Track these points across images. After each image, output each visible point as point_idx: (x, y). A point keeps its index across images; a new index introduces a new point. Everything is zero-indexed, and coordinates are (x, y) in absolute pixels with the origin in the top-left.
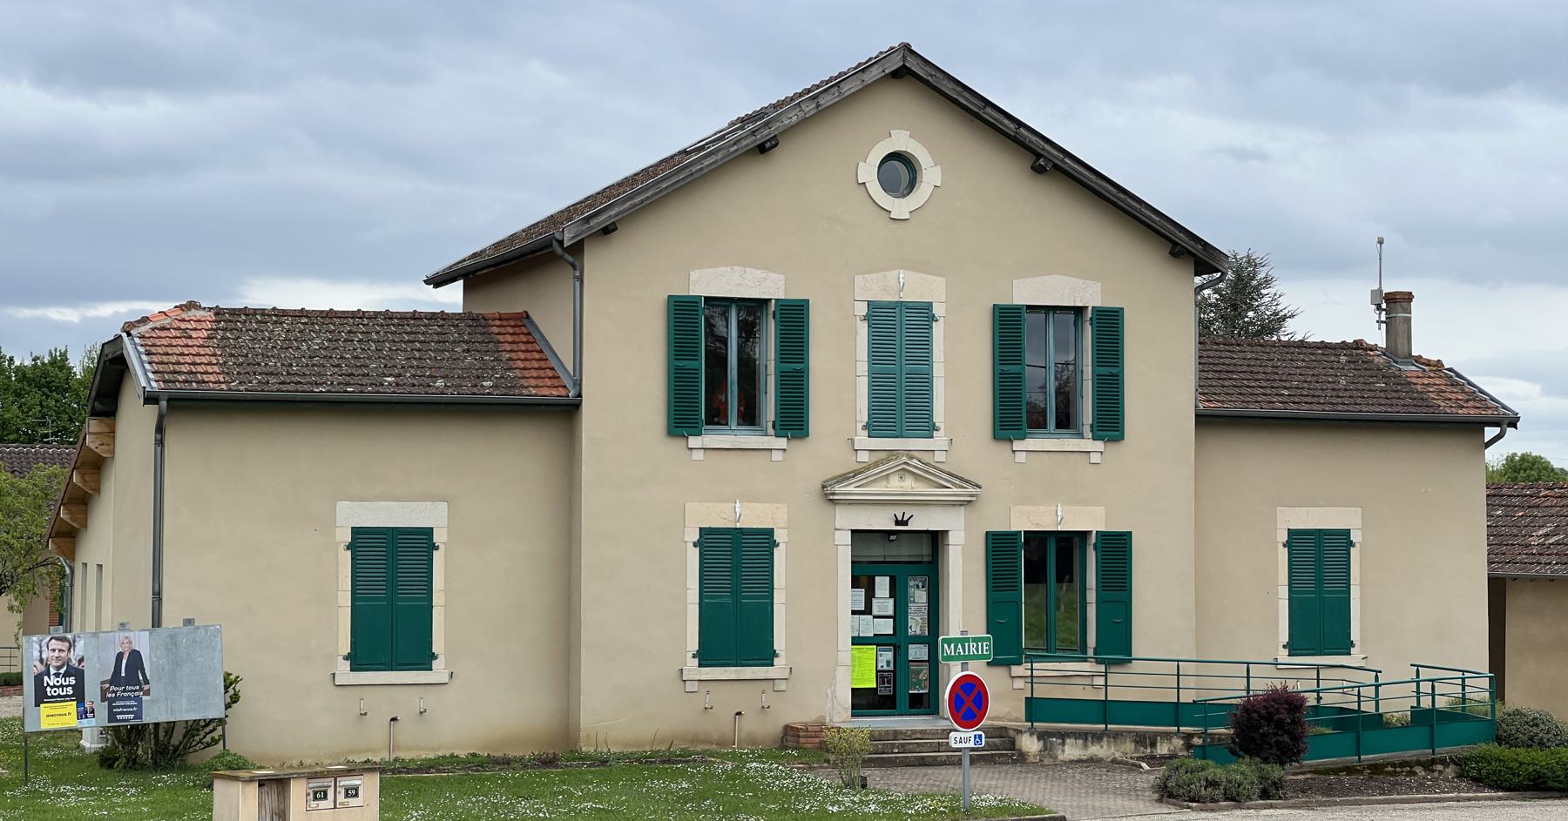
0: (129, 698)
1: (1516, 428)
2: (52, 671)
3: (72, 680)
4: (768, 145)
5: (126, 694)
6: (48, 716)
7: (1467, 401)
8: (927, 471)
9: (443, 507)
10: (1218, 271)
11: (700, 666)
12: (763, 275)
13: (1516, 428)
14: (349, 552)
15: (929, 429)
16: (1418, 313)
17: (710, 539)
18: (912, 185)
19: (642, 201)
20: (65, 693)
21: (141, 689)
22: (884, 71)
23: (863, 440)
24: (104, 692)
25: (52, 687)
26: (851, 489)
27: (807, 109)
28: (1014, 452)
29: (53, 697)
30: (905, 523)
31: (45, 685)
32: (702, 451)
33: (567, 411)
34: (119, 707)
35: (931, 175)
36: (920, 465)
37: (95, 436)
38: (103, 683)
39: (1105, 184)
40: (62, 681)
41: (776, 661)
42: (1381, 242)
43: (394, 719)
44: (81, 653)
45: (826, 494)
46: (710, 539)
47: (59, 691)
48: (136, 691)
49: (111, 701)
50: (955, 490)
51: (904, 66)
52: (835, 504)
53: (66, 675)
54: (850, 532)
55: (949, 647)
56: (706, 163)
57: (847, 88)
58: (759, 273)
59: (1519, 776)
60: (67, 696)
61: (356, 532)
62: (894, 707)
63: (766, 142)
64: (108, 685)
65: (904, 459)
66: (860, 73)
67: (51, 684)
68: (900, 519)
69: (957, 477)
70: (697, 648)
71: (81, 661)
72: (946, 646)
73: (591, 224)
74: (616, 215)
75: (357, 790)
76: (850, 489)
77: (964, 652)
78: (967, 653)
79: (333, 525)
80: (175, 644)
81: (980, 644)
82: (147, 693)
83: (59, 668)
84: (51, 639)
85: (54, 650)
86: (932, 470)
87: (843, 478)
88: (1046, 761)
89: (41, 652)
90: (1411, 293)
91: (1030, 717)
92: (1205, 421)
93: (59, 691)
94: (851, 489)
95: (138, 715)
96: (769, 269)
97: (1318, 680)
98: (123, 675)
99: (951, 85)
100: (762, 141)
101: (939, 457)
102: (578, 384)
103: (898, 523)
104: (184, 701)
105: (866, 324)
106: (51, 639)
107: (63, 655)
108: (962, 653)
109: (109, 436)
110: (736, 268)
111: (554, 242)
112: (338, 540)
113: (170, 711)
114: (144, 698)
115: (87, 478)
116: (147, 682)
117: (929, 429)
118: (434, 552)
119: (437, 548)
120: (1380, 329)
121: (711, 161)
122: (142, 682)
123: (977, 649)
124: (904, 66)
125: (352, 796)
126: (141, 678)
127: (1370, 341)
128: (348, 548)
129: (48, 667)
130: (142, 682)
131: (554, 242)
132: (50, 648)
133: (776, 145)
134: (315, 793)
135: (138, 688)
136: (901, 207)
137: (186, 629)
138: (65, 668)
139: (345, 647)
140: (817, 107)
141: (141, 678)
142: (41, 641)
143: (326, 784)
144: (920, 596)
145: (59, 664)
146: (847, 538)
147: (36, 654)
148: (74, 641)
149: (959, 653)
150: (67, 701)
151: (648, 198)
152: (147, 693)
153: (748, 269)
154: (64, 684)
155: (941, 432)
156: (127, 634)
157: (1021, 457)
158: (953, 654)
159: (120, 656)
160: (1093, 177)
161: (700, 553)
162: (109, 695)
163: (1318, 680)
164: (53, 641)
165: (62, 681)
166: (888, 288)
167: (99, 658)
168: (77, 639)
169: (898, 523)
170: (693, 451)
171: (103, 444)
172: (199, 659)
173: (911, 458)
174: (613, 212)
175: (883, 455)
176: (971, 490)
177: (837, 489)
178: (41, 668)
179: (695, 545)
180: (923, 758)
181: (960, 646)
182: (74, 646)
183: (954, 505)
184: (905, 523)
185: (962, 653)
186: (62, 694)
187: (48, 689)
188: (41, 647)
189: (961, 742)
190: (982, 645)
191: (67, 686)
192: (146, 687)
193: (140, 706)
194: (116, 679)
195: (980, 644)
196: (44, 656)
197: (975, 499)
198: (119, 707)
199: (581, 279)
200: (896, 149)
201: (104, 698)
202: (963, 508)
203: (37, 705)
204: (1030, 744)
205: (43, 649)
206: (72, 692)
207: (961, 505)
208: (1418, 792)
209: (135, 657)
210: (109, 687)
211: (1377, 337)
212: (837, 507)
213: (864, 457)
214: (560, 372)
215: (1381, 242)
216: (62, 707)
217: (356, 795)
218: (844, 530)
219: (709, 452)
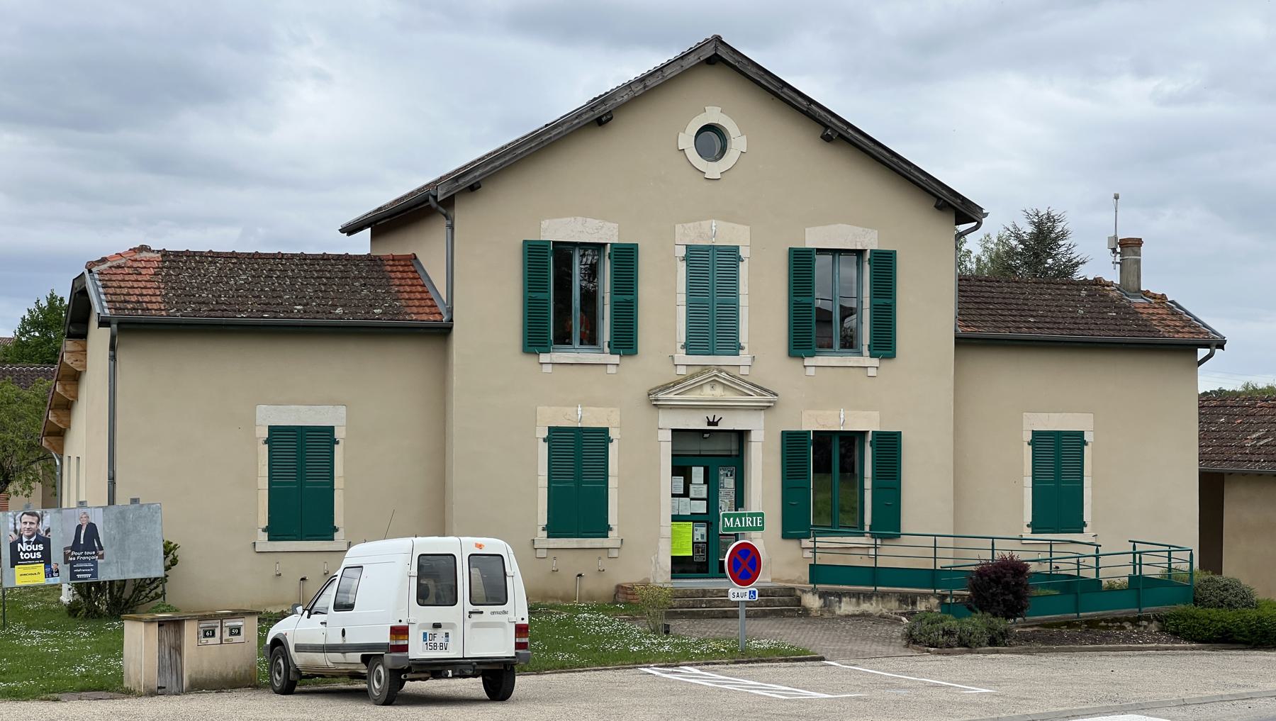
0: (87, 561)
1: (1223, 349)
2: (25, 539)
3: (41, 547)
4: (604, 119)
5: (84, 558)
7: (1183, 327)
8: (734, 382)
9: (342, 410)
10: (974, 221)
11: (548, 537)
12: (601, 224)
13: (1223, 349)
15: (736, 349)
17: (557, 436)
18: (723, 151)
19: (501, 165)
20: (35, 557)
21: (96, 554)
23: (681, 357)
24: (66, 556)
25: (24, 552)
26: (671, 396)
27: (636, 90)
28: (805, 366)
29: (25, 560)
30: (716, 424)
31: (19, 550)
33: (442, 332)
34: (79, 568)
35: (738, 143)
37: (70, 354)
38: (65, 549)
39: (880, 150)
40: (32, 547)
41: (610, 533)
42: (1117, 197)
43: (303, 579)
44: (48, 525)
45: (651, 401)
46: (557, 436)
47: (30, 555)
48: (91, 555)
49: (72, 563)
50: (756, 397)
51: (716, 54)
52: (659, 408)
53: (36, 543)
55: (729, 520)
56: (554, 134)
57: (669, 72)
58: (597, 223)
59: (1209, 630)
60: (36, 559)
61: (273, 430)
62: (707, 572)
63: (602, 116)
64: (69, 551)
65: (715, 372)
66: (679, 60)
67: (24, 550)
68: (711, 420)
69: (758, 387)
70: (546, 523)
71: (48, 531)
72: (726, 519)
73: (460, 183)
74: (480, 175)
75: (239, 629)
76: (671, 396)
77: (741, 524)
78: (743, 526)
79: (253, 424)
80: (124, 519)
81: (754, 518)
82: (102, 557)
83: (30, 537)
84: (23, 515)
85: (26, 523)
86: (737, 381)
87: (665, 388)
88: (826, 615)
89: (15, 524)
90: (1141, 239)
91: (813, 580)
92: (962, 342)
93: (30, 555)
94: (671, 396)
95: (94, 574)
96: (605, 219)
97: (1051, 552)
98: (82, 542)
99: (755, 70)
100: (599, 116)
101: (744, 371)
102: (451, 311)
103: (710, 424)
104: (131, 563)
105: (684, 264)
106: (23, 515)
107: (33, 526)
108: (740, 526)
109: (82, 354)
111: (430, 198)
112: (257, 436)
113: (120, 571)
114: (99, 561)
115: (68, 388)
116: (101, 548)
117: (736, 349)
118: (335, 446)
119: (338, 443)
120: (1115, 269)
121: (560, 130)
122: (97, 548)
123: (752, 522)
124: (716, 54)
125: (235, 634)
126: (96, 545)
127: (1108, 279)
128: (266, 443)
129: (21, 536)
130: (97, 548)
131: (430, 198)
132: (23, 521)
133: (611, 118)
134: (205, 632)
135: (94, 553)
136: (713, 169)
137: (133, 506)
138: (35, 537)
139: (264, 521)
140: (645, 87)
141: (96, 545)
142: (15, 516)
143: (213, 625)
144: (729, 483)
145: (30, 534)
146: (668, 436)
147: (11, 526)
148: (42, 516)
149: (737, 525)
150: (37, 563)
151: (505, 162)
152: (102, 557)
153: (588, 219)
154: (34, 550)
155: (746, 351)
156: (85, 510)
157: (811, 371)
158: (732, 526)
159: (79, 528)
160: (871, 144)
162: (71, 559)
163: (1051, 552)
164: (25, 515)
165: (32, 547)
166: (703, 235)
167: (62, 530)
168: (45, 514)
169: (710, 424)
170: (544, 366)
171: (77, 361)
172: (143, 531)
173: (721, 371)
174: (477, 174)
175: (698, 369)
176: (769, 397)
177: (660, 396)
178: (16, 537)
179: (544, 440)
180: (725, 611)
181: (738, 519)
182: (42, 520)
183: (755, 409)
184: (716, 424)
185: (740, 526)
186: (32, 557)
187: (21, 554)
188: (15, 521)
189: (738, 596)
190: (756, 519)
191: (36, 552)
192: (100, 553)
193: (96, 567)
194: (76, 546)
195: (754, 518)
196: (18, 528)
197: (772, 404)
198: (79, 568)
199: (452, 227)
200: (710, 122)
201: (66, 562)
202: (763, 411)
203: (13, 566)
204: (812, 602)
205: (17, 522)
206: (40, 556)
208: (1124, 642)
209: (92, 529)
210: (71, 553)
211: (1112, 275)
212: (660, 411)
213: (682, 371)
214: (437, 302)
215: (1117, 197)
216: (33, 568)
217: (239, 633)
218: (666, 429)
219: (556, 366)
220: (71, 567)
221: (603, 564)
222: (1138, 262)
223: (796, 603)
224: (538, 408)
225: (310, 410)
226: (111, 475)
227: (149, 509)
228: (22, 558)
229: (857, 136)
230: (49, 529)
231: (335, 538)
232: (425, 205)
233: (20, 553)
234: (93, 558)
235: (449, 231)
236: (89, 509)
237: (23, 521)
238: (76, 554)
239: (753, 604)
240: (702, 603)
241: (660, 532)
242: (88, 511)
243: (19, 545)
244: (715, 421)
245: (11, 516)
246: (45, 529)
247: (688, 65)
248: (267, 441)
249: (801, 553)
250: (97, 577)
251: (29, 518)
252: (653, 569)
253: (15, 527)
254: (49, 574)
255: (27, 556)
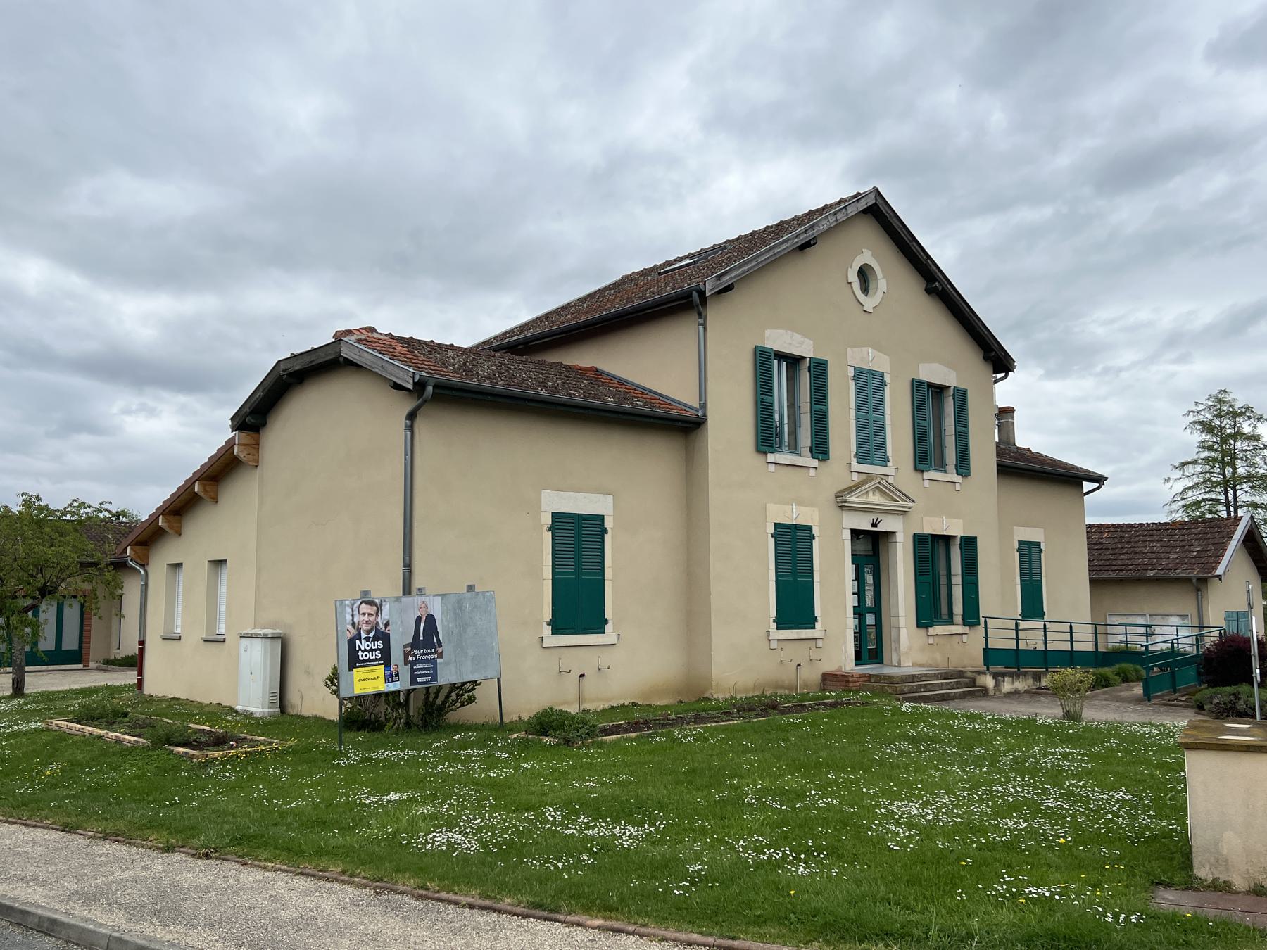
0: (426, 661)
2: (363, 635)
3: (380, 644)
4: (812, 242)
5: (424, 657)
6: (360, 680)
14: (550, 533)
19: (749, 270)
20: (374, 657)
21: (436, 652)
22: (867, 204)
24: (406, 655)
25: (363, 651)
26: (853, 499)
29: (364, 661)
31: (357, 649)
32: (774, 465)
34: (419, 670)
35: (881, 283)
36: (887, 485)
37: (243, 447)
38: (405, 646)
40: (371, 645)
43: (582, 676)
44: (387, 617)
45: (838, 502)
47: (369, 655)
48: (432, 654)
49: (413, 663)
50: (901, 503)
52: (842, 510)
53: (375, 639)
54: (850, 531)
56: (782, 248)
57: (840, 216)
60: (376, 660)
61: (555, 516)
63: (811, 240)
64: (409, 649)
65: (879, 480)
67: (363, 649)
71: (387, 624)
73: (721, 281)
74: (735, 277)
79: (538, 510)
80: (460, 608)
82: (440, 656)
83: (368, 632)
84: (361, 604)
85: (364, 614)
86: (892, 489)
87: (850, 490)
88: (997, 693)
89: (353, 616)
91: (987, 663)
93: (369, 655)
95: (434, 678)
96: (805, 336)
98: (421, 638)
104: (469, 663)
106: (361, 604)
107: (372, 618)
109: (254, 448)
110: (789, 332)
111: (695, 294)
113: (458, 673)
114: (439, 660)
115: (208, 488)
116: (440, 645)
122: (436, 645)
126: (436, 642)
128: (550, 530)
129: (359, 630)
130: (436, 645)
131: (695, 294)
132: (361, 612)
135: (433, 650)
137: (469, 594)
138: (374, 632)
139: (548, 615)
140: (837, 220)
141: (436, 642)
142: (353, 605)
144: (869, 579)
145: (369, 628)
147: (349, 618)
148: (381, 605)
150: (376, 665)
151: (751, 268)
152: (440, 656)
154: (373, 648)
156: (423, 599)
157: (927, 483)
159: (418, 620)
162: (411, 659)
163: (1071, 632)
164: (363, 605)
165: (371, 645)
167: (402, 622)
168: (384, 604)
171: (249, 454)
172: (479, 623)
173: (882, 479)
174: (733, 275)
176: (910, 503)
177: (848, 498)
178: (353, 632)
180: (943, 694)
182: (381, 610)
183: (898, 514)
186: (371, 658)
187: (360, 653)
188: (353, 611)
191: (376, 650)
192: (440, 650)
193: (435, 669)
194: (415, 643)
196: (356, 620)
198: (419, 670)
201: (406, 662)
202: (902, 516)
203: (351, 669)
204: (989, 681)
205: (355, 613)
206: (380, 656)
209: (431, 619)
210: (410, 651)
216: (372, 671)
219: (778, 466)
220: (411, 668)
221: (814, 654)
222: (1013, 423)
223: (972, 684)
224: (768, 505)
225: (585, 498)
226: (407, 561)
227: (484, 597)
228: (361, 659)
229: (954, 293)
230: (389, 621)
231: (816, 627)
232: (665, 306)
233: (358, 652)
234: (433, 657)
235: (701, 329)
236: (428, 598)
237: (361, 612)
238: (416, 652)
239: (949, 687)
240: (921, 688)
241: (846, 624)
242: (427, 599)
243: (358, 642)
245: (348, 606)
246: (384, 623)
247: (346, 354)
248: (550, 529)
249: (926, 640)
250: (437, 681)
251: (368, 609)
252: (844, 658)
253: (353, 620)
254: (389, 678)
255: (366, 656)
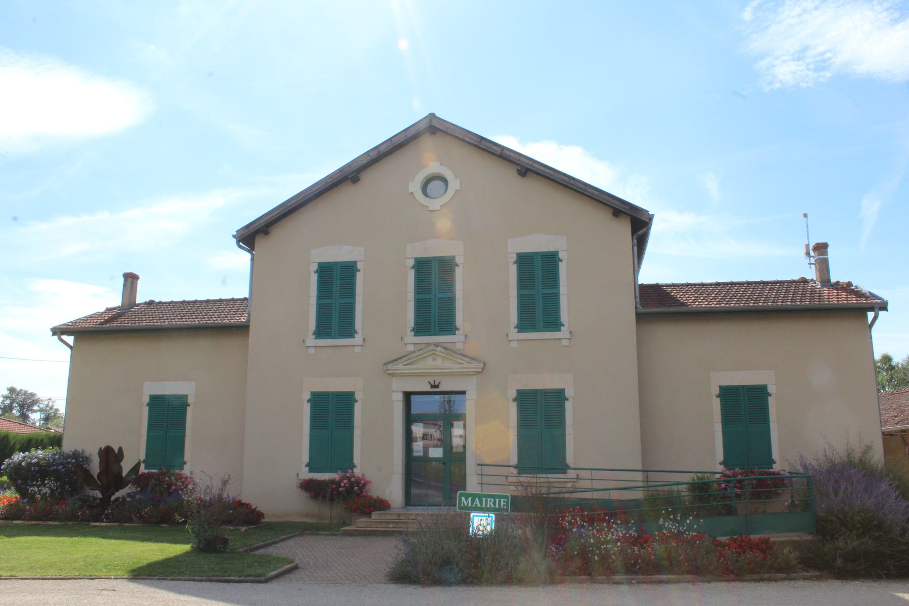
9: (193, 384)
16: (832, 254)
23: (411, 338)
30: (437, 387)
42: (805, 216)
52: (393, 376)
54: (402, 393)
63: (349, 175)
68: (433, 384)
76: (400, 367)
90: (827, 243)
92: (641, 318)
94: (400, 366)
101: (459, 346)
103: (432, 387)
120: (810, 268)
127: (809, 278)
157: (514, 344)
161: (311, 406)
169: (432, 387)
175: (422, 346)
177: (390, 366)
183: (469, 375)
184: (437, 387)
202: (475, 377)
207: (474, 375)
211: (811, 274)
212: (394, 378)
213: (411, 348)
215: (805, 216)
244: (436, 384)
248: (148, 405)
